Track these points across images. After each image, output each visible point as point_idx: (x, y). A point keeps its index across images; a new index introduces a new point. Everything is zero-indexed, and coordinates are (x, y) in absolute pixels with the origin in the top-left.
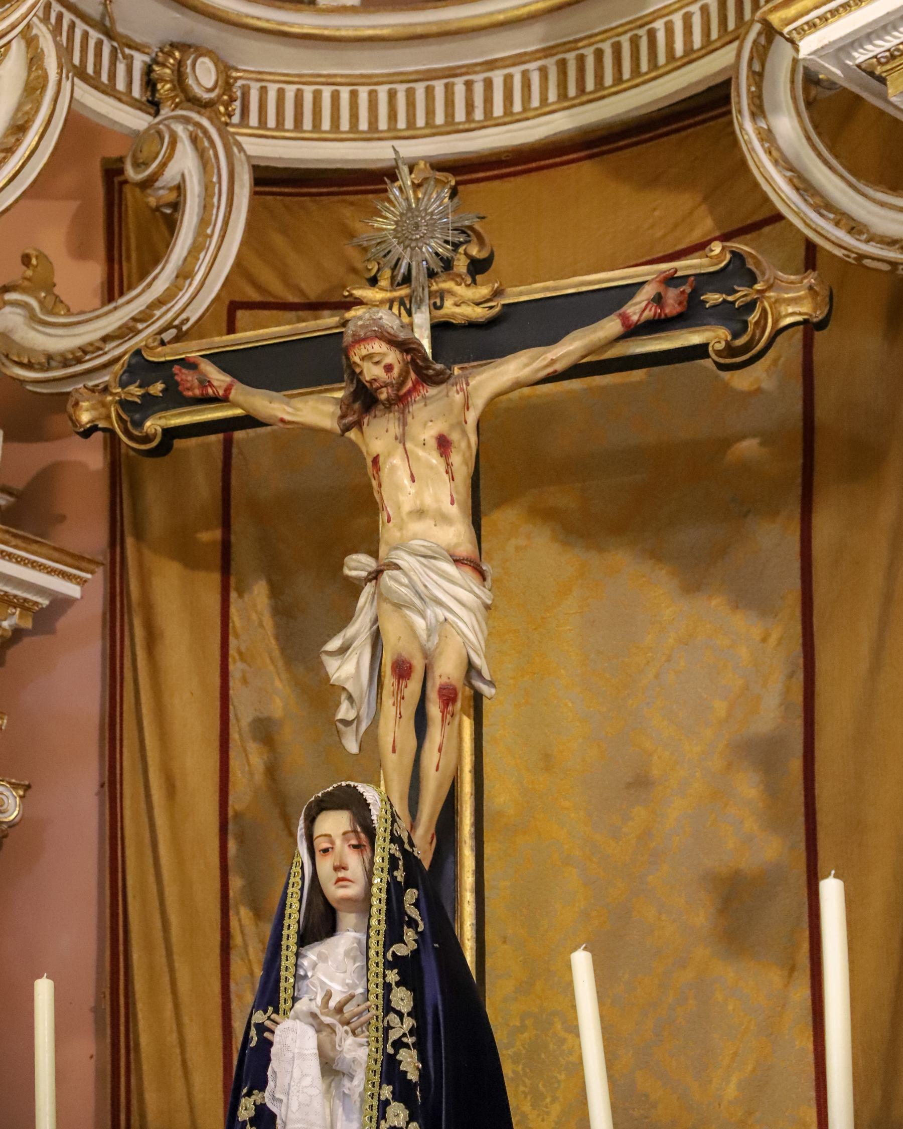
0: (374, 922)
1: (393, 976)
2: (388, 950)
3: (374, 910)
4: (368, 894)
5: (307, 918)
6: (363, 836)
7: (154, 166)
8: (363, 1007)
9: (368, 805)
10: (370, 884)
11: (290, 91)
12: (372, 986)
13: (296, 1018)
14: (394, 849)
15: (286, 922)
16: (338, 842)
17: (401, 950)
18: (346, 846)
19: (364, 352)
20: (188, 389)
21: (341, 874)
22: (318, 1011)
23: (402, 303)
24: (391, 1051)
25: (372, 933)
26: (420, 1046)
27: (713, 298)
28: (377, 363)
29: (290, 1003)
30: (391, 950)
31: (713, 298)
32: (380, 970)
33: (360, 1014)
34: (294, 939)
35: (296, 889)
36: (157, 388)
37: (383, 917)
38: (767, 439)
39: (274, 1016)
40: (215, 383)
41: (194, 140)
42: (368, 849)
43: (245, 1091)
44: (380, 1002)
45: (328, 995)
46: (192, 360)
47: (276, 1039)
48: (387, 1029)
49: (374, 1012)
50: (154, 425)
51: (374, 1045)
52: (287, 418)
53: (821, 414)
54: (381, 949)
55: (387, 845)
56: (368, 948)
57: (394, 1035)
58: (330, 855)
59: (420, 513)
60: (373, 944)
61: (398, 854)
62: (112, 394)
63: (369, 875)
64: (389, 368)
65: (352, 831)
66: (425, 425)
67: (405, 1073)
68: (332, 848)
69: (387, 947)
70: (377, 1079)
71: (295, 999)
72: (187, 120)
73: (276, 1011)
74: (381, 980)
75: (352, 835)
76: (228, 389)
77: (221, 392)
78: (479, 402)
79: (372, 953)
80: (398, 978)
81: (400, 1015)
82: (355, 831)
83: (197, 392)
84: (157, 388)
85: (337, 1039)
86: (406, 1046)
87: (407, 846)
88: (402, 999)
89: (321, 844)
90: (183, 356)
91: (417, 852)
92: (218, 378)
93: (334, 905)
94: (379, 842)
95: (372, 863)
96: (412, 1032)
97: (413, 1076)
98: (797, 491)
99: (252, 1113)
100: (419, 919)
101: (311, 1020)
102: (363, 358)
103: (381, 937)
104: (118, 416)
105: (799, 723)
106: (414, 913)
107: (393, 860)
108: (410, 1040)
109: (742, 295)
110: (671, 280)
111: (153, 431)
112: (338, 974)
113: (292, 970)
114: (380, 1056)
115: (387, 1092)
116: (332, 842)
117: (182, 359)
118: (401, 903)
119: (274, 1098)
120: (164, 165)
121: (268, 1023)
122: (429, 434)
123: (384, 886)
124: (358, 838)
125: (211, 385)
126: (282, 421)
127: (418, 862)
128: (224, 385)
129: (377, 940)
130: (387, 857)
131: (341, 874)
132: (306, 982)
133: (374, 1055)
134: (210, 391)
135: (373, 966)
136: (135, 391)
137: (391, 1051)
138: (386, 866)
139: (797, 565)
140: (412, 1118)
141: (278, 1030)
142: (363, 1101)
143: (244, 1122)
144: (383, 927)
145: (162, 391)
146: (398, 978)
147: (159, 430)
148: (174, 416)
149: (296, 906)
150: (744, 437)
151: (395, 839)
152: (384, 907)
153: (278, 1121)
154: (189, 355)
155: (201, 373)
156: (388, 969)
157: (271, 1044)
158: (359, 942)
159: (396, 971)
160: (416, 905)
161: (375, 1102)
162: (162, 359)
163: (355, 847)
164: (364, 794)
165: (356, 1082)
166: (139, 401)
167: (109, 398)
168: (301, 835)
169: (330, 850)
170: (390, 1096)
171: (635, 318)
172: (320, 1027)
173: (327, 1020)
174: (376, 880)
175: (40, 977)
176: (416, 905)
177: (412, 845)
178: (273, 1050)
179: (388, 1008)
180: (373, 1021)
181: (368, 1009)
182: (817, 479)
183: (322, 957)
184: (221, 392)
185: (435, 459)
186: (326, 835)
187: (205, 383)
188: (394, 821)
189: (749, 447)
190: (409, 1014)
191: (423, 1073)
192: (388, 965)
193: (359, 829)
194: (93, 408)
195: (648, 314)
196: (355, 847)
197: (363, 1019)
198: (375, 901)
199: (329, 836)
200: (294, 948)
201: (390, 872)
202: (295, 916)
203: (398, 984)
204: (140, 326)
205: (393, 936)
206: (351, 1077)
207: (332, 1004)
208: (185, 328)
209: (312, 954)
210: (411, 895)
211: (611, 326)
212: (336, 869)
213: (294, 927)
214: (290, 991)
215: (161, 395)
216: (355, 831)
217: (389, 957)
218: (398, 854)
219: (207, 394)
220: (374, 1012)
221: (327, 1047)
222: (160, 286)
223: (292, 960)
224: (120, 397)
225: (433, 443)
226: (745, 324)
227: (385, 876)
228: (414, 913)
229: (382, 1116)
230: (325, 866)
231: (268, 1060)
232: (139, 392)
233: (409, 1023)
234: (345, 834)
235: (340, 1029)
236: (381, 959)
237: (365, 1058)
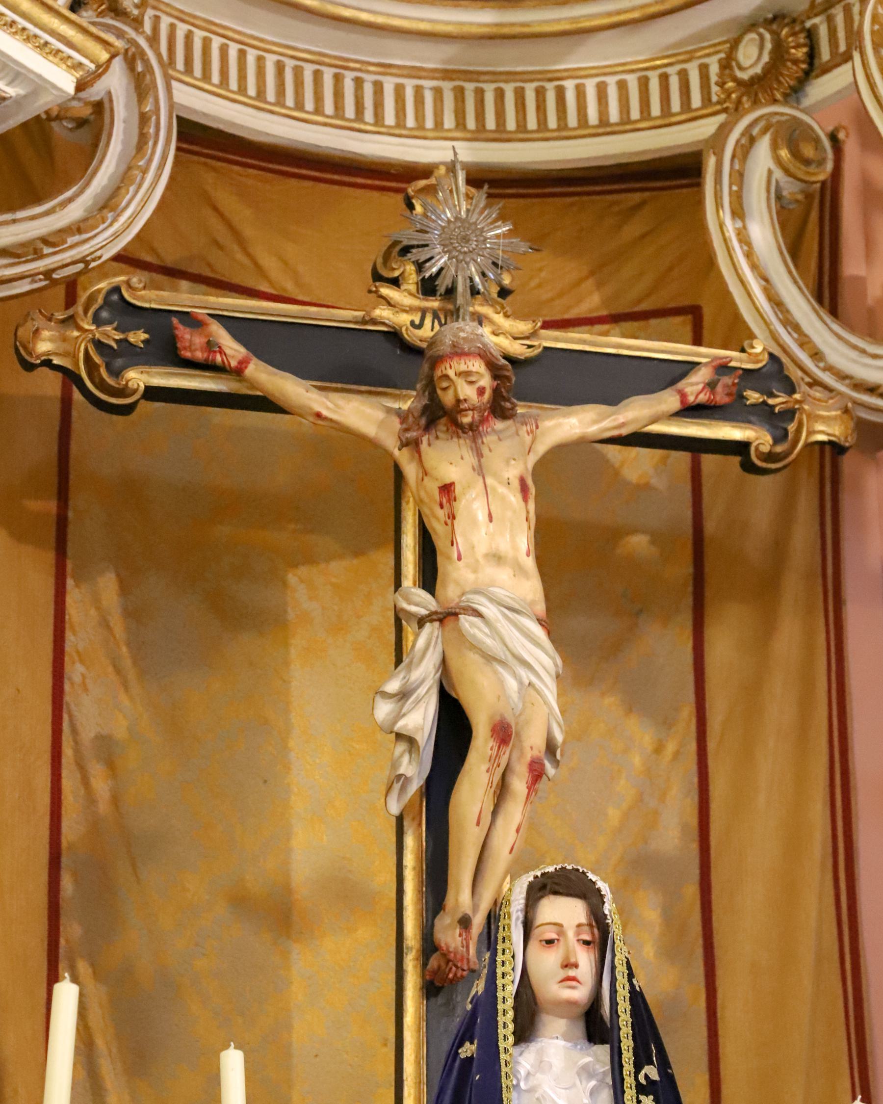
2: (640, 1071)
6: (596, 931)
9: (602, 897)
16: (571, 934)
18: (575, 942)
19: (463, 367)
20: (185, 348)
21: (572, 973)
23: (436, 316)
27: (753, 397)
28: (472, 383)
30: (643, 1073)
31: (753, 397)
34: (511, 1039)
36: (138, 337)
38: (656, 538)
40: (228, 351)
46: (201, 317)
52: (325, 413)
53: (710, 527)
58: (555, 948)
59: (497, 558)
62: (79, 328)
64: (481, 391)
65: (587, 925)
66: (507, 463)
68: (558, 940)
69: (638, 1067)
75: (587, 928)
76: (244, 363)
77: (234, 363)
78: (541, 448)
83: (200, 355)
84: (138, 337)
98: (689, 601)
102: (459, 374)
104: (87, 357)
105: (695, 846)
109: (779, 401)
110: (723, 368)
111: (135, 386)
112: (558, 1089)
117: (187, 313)
125: (221, 352)
126: (318, 415)
128: (240, 357)
131: (572, 973)
134: (218, 358)
136: (111, 335)
139: (690, 678)
145: (145, 342)
148: (159, 374)
150: (635, 531)
155: (210, 335)
156: (642, 1094)
159: (651, 1097)
162: (147, 305)
163: (587, 943)
164: (597, 882)
166: (115, 346)
167: (76, 333)
168: (517, 919)
169: (556, 941)
171: (691, 399)
182: (709, 593)
183: (541, 1065)
184: (234, 363)
186: (555, 924)
187: (211, 346)
189: (639, 543)
193: (594, 924)
194: (51, 340)
195: (703, 398)
196: (587, 943)
199: (560, 925)
211: (669, 401)
216: (590, 925)
217: (643, 1081)
219: (214, 360)
225: (516, 484)
226: (786, 431)
234: (579, 926)
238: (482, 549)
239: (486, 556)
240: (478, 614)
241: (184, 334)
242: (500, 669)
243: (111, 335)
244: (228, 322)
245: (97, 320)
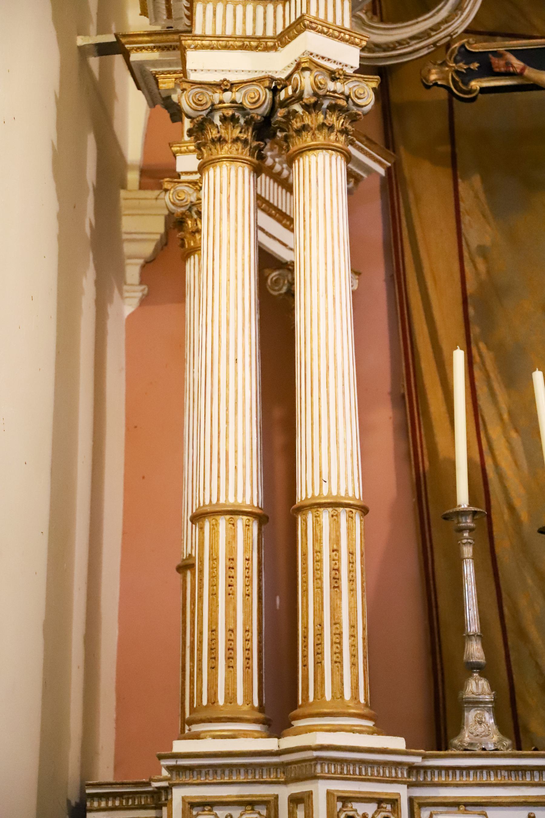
20: (497, 67)
36: (475, 66)
40: (515, 65)
46: (502, 52)
50: (476, 84)
76: (523, 69)
77: (518, 71)
83: (503, 69)
84: (475, 66)
90: (495, 50)
92: (517, 64)
111: (475, 88)
117: (496, 52)
125: (513, 66)
128: (521, 67)
134: (511, 69)
136: (462, 67)
145: (478, 67)
147: (478, 88)
148: (485, 81)
154: (499, 49)
155: (506, 59)
162: (477, 51)
166: (464, 71)
167: (447, 69)
175: (535, 370)
184: (518, 71)
187: (508, 64)
204: (433, 33)
208: (454, 36)
215: (477, 69)
219: (509, 71)
222: (444, 14)
224: (455, 68)
232: (465, 67)
241: (495, 61)
243: (462, 67)
244: (515, 52)
245: (456, 62)
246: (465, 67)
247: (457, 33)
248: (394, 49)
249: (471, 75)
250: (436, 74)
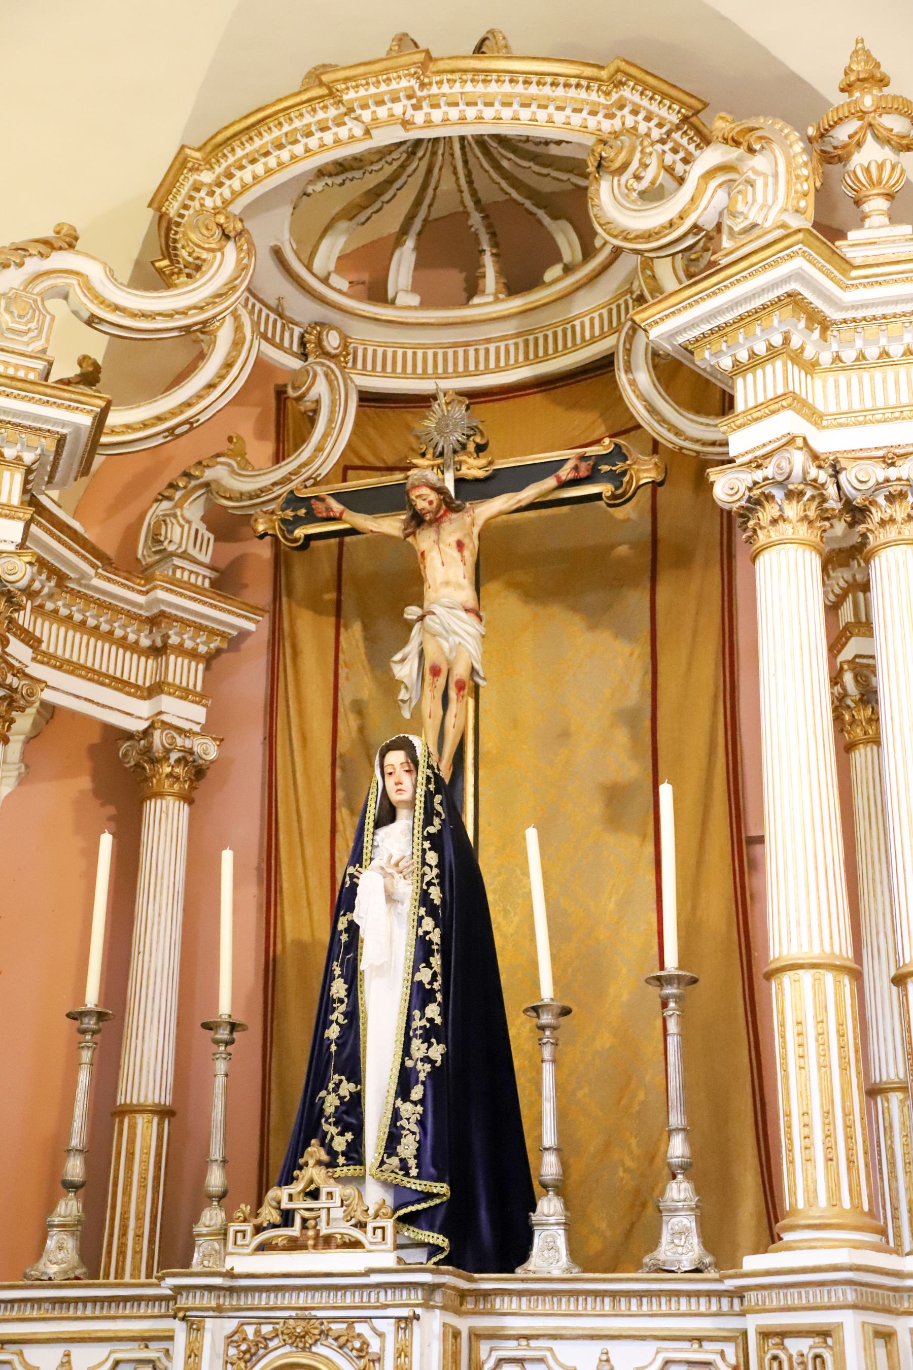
0: (417, 814)
1: (427, 845)
3: (417, 808)
4: (414, 798)
5: (379, 813)
6: (412, 765)
7: (304, 389)
8: (410, 862)
10: (415, 792)
11: (380, 351)
12: (415, 851)
13: (372, 870)
14: (429, 772)
15: (368, 815)
17: (432, 830)
19: (418, 493)
21: (399, 787)
22: (384, 866)
23: (439, 467)
24: (425, 887)
25: (416, 820)
26: (441, 885)
27: (605, 468)
28: (424, 500)
29: (369, 861)
31: (605, 468)
32: (420, 841)
33: (408, 867)
34: (372, 824)
35: (374, 796)
37: (422, 811)
39: (360, 869)
40: (335, 510)
41: (326, 375)
42: (415, 772)
43: (342, 913)
44: (420, 860)
45: (391, 857)
47: (360, 882)
48: (423, 875)
49: (416, 865)
51: (416, 884)
52: (374, 529)
54: (421, 829)
55: (425, 770)
56: (413, 829)
57: (427, 879)
59: (447, 583)
60: (416, 826)
61: (431, 775)
63: (415, 787)
64: (431, 503)
66: (450, 534)
67: (433, 900)
69: (424, 828)
70: (417, 904)
71: (371, 859)
72: (323, 364)
73: (361, 866)
74: (420, 847)
76: (341, 513)
77: (338, 515)
78: (480, 522)
79: (416, 832)
80: (429, 846)
81: (431, 867)
82: (407, 762)
83: (324, 515)
85: (395, 881)
86: (434, 884)
87: (436, 771)
88: (432, 858)
89: (388, 770)
91: (442, 774)
93: (395, 804)
94: (420, 768)
95: (416, 780)
96: (437, 877)
97: (437, 902)
99: (346, 926)
100: (442, 812)
101: (380, 871)
102: (417, 497)
103: (421, 823)
106: (439, 808)
107: (428, 778)
108: (436, 881)
110: (583, 458)
113: (370, 842)
114: (419, 891)
115: (422, 911)
116: (394, 769)
118: (432, 802)
119: (358, 916)
120: (309, 389)
121: (356, 873)
122: (452, 540)
123: (423, 793)
124: (409, 766)
125: (332, 510)
126: (372, 531)
127: (442, 779)
129: (419, 824)
130: (425, 777)
132: (378, 849)
133: (416, 890)
134: (332, 514)
135: (415, 839)
137: (425, 887)
138: (424, 782)
140: (436, 926)
141: (361, 877)
142: (409, 917)
143: (341, 931)
144: (422, 817)
146: (429, 846)
149: (373, 805)
151: (430, 767)
152: (423, 805)
153: (361, 930)
157: (357, 885)
158: (409, 826)
160: (441, 804)
161: (416, 918)
163: (407, 771)
165: (405, 905)
170: (424, 914)
171: (564, 478)
172: (386, 875)
173: (389, 870)
174: (418, 790)
176: (441, 804)
177: (439, 770)
178: (358, 889)
179: (424, 863)
180: (416, 871)
181: (413, 864)
184: (338, 515)
185: (455, 554)
187: (329, 509)
188: (429, 757)
190: (436, 866)
191: (443, 900)
192: (425, 839)
195: (571, 476)
196: (407, 771)
197: (410, 870)
198: (417, 802)
200: (371, 830)
201: (427, 786)
202: (373, 811)
203: (430, 849)
205: (428, 822)
206: (403, 903)
207: (393, 861)
209: (383, 832)
210: (438, 798)
211: (550, 482)
212: (397, 784)
213: (372, 818)
214: (369, 855)
216: (407, 762)
217: (425, 834)
218: (431, 775)
220: (416, 865)
221: (390, 887)
223: (371, 836)
225: (454, 545)
226: (622, 482)
227: (424, 788)
228: (439, 808)
229: (420, 925)
230: (390, 783)
231: (356, 894)
233: (436, 871)
235: (397, 876)
236: (420, 835)
237: (411, 892)
238: (439, 580)
239: (442, 583)
240: (434, 614)
241: (319, 506)
242: (439, 639)
243: (289, 514)
244: (337, 496)
245: (283, 510)
246: (292, 514)
247: (320, 474)
248: (258, 497)
249: (298, 521)
250: (265, 523)
